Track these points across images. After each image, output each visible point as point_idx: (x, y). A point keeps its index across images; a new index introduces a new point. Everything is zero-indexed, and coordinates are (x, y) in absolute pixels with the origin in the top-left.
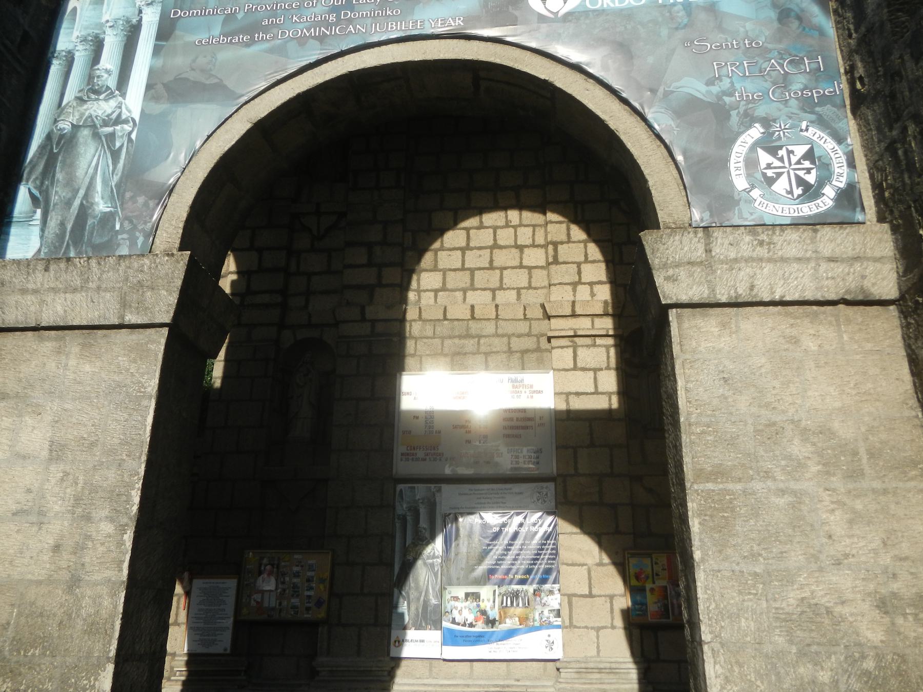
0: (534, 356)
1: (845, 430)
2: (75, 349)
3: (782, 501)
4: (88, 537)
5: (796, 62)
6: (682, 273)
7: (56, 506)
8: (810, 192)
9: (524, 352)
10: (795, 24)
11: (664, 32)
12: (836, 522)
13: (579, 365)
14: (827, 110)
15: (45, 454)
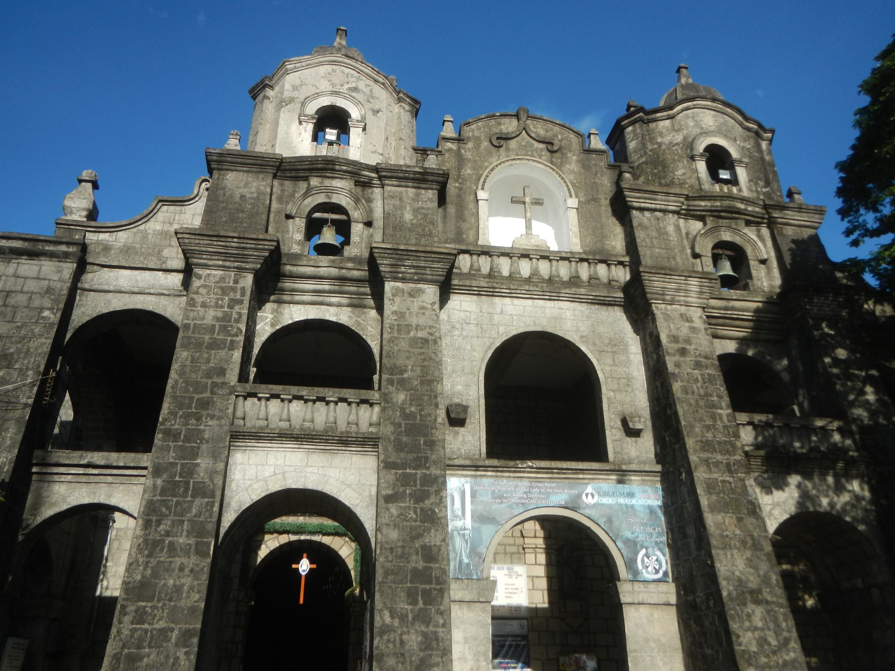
0: (517, 556)
1: (663, 640)
2: (465, 608)
3: (649, 659)
4: (479, 666)
5: (654, 529)
6: (627, 595)
7: (469, 657)
8: (657, 572)
9: (512, 554)
10: (654, 515)
11: (620, 514)
12: (660, 664)
13: (538, 562)
14: (661, 546)
15: (462, 641)
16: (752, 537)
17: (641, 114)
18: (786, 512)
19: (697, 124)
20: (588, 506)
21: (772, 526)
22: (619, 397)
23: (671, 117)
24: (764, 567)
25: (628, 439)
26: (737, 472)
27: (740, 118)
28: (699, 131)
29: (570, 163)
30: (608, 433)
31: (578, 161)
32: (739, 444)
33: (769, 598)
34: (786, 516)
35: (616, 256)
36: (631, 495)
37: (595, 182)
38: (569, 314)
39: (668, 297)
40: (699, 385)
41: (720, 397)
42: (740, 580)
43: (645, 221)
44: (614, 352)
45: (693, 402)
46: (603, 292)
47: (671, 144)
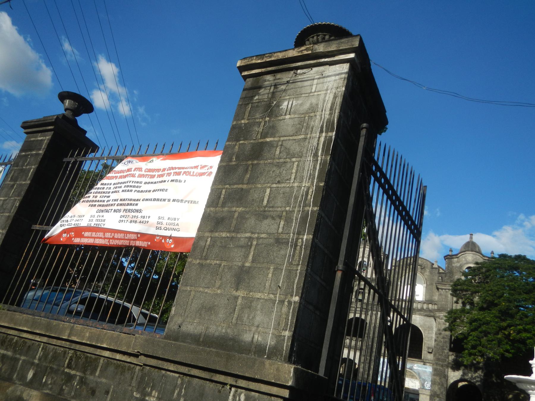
16: (442, 383)
17: (448, 257)
18: (457, 378)
19: (466, 260)
20: (414, 369)
21: (451, 381)
22: (428, 342)
23: (458, 258)
24: (442, 390)
25: (428, 354)
26: (444, 367)
27: (482, 256)
28: (465, 262)
29: (426, 272)
30: (423, 352)
31: (429, 271)
32: (447, 360)
33: (441, 397)
34: (456, 379)
35: (434, 302)
36: (426, 368)
37: (433, 278)
38: (418, 319)
39: (440, 318)
40: (442, 343)
41: (447, 347)
42: (435, 392)
43: (442, 293)
44: (429, 330)
45: (438, 348)
46: (428, 313)
47: (456, 267)
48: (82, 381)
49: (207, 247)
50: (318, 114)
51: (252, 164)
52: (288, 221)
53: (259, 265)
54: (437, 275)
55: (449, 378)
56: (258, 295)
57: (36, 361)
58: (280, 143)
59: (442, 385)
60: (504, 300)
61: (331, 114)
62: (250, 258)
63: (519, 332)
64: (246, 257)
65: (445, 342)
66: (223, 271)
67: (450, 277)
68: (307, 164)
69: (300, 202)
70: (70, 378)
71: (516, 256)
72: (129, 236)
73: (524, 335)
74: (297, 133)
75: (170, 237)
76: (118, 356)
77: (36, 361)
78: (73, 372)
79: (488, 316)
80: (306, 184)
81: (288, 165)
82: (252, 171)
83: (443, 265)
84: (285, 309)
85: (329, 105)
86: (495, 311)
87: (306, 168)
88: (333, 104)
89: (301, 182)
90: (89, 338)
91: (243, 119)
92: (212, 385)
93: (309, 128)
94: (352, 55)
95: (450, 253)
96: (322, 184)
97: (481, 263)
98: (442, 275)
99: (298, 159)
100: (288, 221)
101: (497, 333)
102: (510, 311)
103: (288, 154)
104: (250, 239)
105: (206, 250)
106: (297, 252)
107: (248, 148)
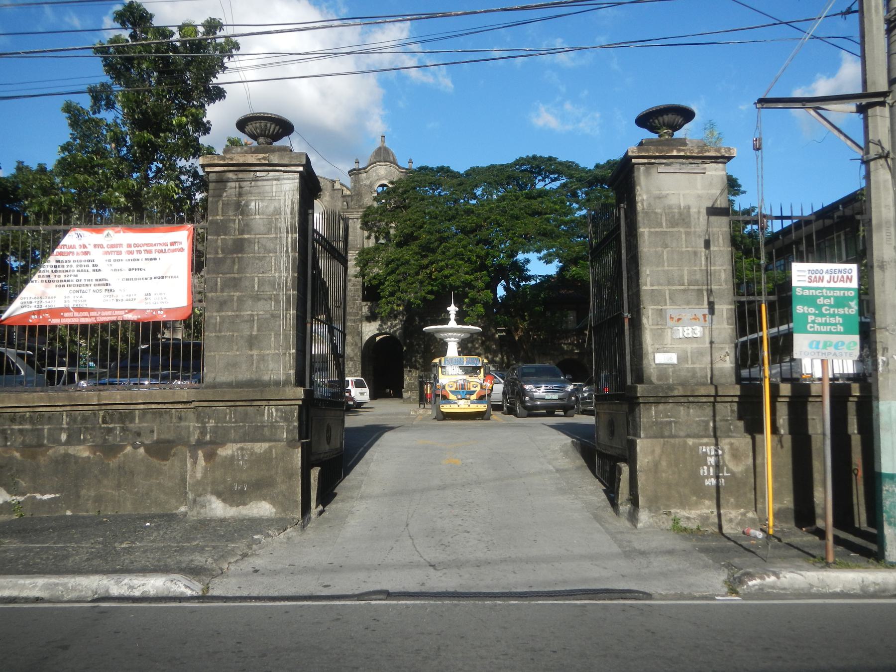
21: (366, 338)
28: (377, 178)
47: (365, 185)
48: (123, 429)
49: (218, 323)
50: (282, 216)
51: (238, 257)
52: (277, 301)
53: (263, 333)
54: (341, 199)
55: (364, 335)
56: (268, 352)
57: (65, 426)
58: (257, 240)
59: (356, 345)
60: (424, 231)
61: (292, 218)
62: (255, 328)
63: (441, 269)
64: (252, 328)
65: (357, 290)
66: (237, 339)
67: (358, 201)
68: (282, 258)
69: (283, 287)
70: (110, 431)
71: (438, 168)
72: (117, 313)
73: (447, 272)
74: (269, 232)
75: (161, 310)
76: (153, 406)
77: (65, 426)
78: (111, 426)
79: (406, 254)
80: (284, 274)
81: (268, 259)
82: (239, 262)
83: (348, 181)
84: (287, 358)
85: (289, 210)
86: (414, 247)
87: (282, 262)
88: (292, 209)
89: (280, 272)
90: (121, 399)
91: (218, 215)
92: (252, 408)
93: (278, 229)
94: (301, 169)
95: (355, 166)
96: (296, 275)
97: (396, 182)
98: (347, 198)
99: (274, 255)
100: (277, 301)
101: (417, 274)
102: (432, 246)
103: (265, 249)
104: (252, 315)
105: (218, 326)
106: (288, 322)
107: (230, 243)
